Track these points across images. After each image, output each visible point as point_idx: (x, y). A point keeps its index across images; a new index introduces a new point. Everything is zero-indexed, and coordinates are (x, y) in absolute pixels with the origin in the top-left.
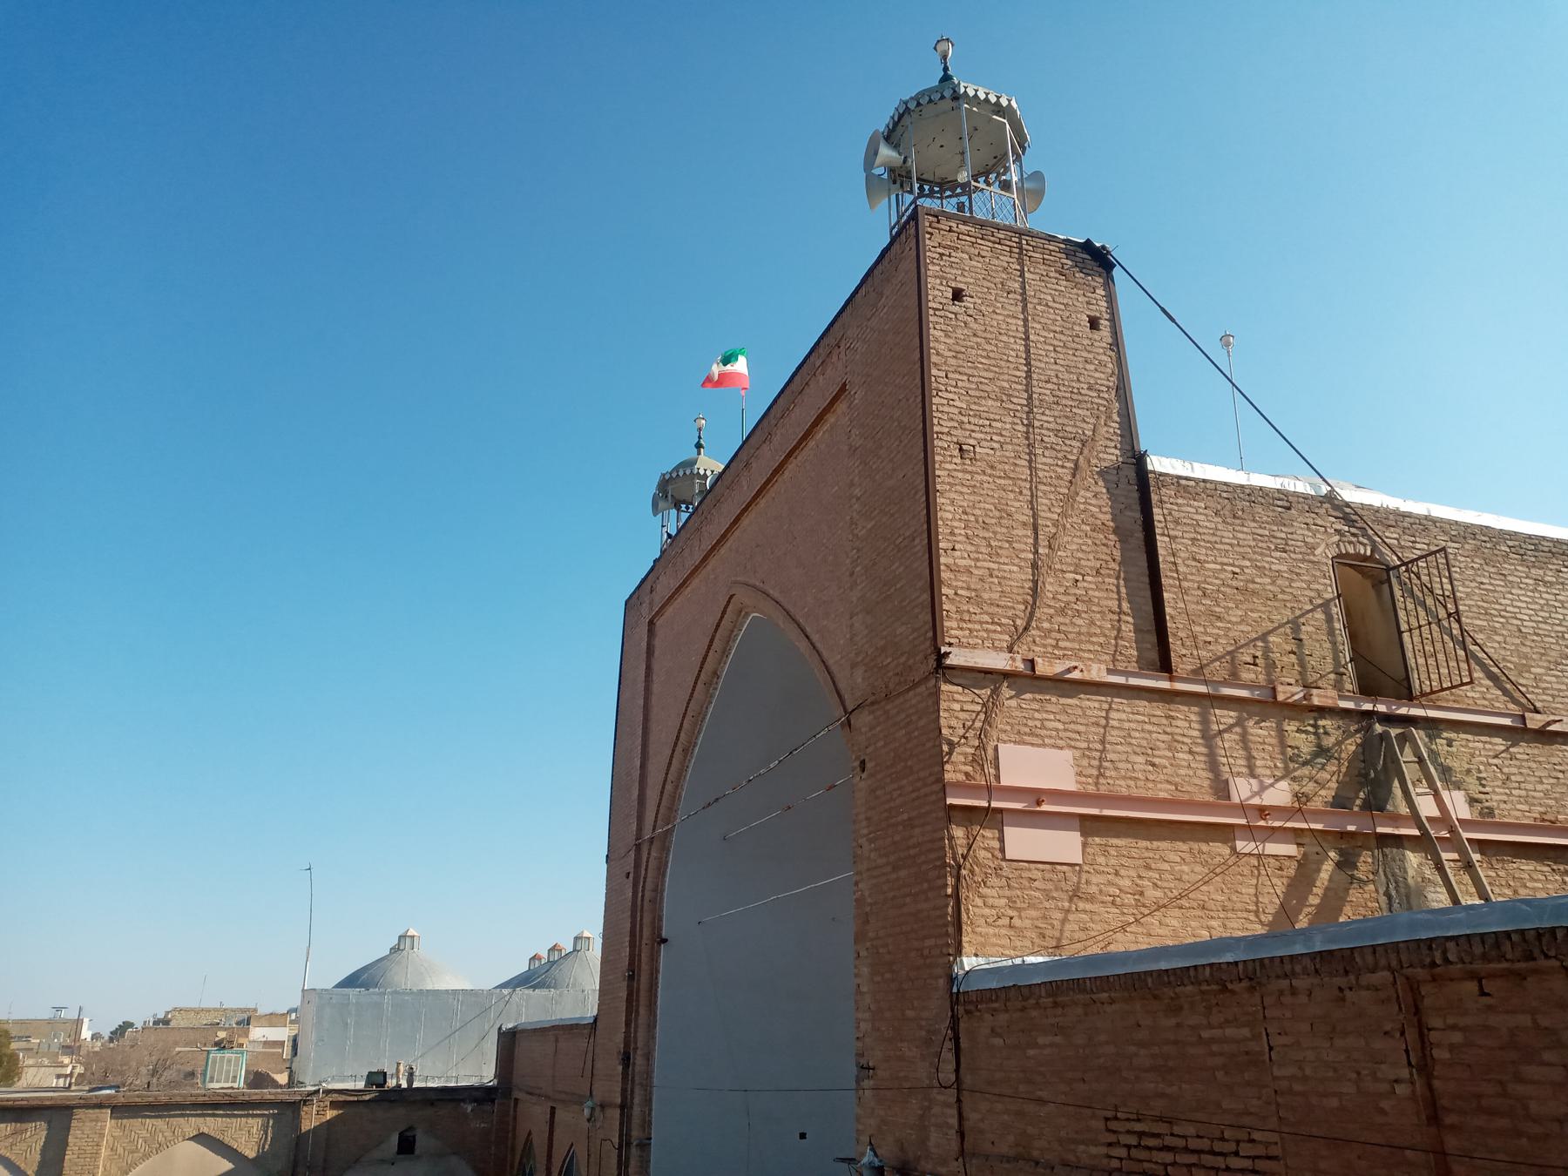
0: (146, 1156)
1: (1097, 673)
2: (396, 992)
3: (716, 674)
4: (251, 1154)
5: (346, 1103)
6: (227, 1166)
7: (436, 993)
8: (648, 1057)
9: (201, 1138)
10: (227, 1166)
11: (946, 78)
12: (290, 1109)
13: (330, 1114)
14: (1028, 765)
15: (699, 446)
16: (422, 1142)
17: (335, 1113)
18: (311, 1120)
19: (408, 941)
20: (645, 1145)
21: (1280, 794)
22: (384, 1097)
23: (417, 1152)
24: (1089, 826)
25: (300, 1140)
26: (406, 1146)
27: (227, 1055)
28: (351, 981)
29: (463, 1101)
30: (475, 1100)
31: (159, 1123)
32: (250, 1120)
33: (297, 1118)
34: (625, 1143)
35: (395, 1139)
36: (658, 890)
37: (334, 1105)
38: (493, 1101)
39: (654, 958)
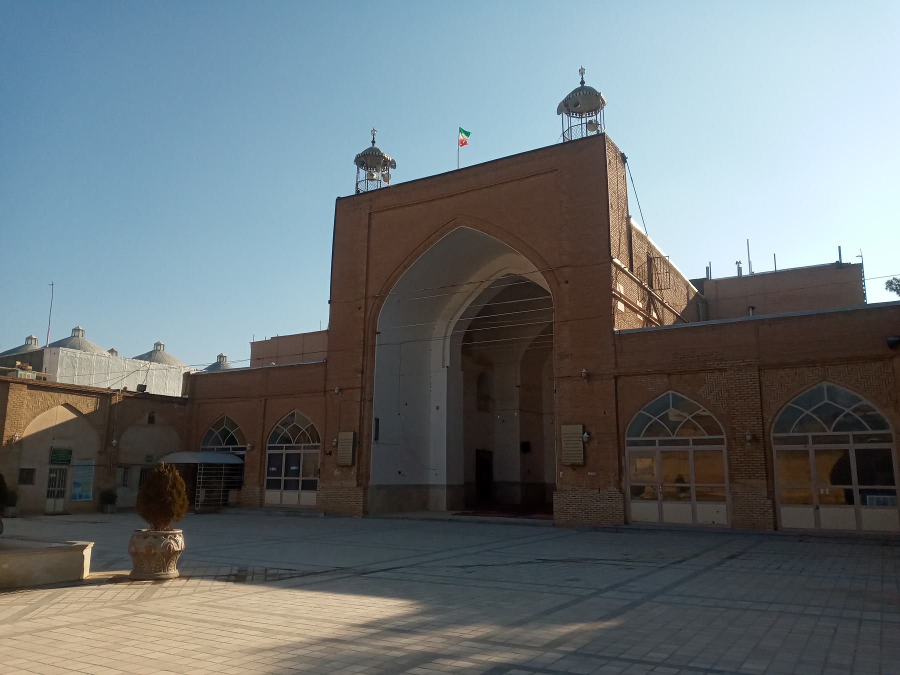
1: (626, 269)
3: (432, 243)
8: (372, 370)
9: (67, 405)
11: (582, 82)
12: (104, 396)
14: (620, 288)
15: (373, 142)
20: (371, 400)
21: (640, 305)
24: (626, 305)
26: (151, 420)
34: (363, 400)
35: (147, 416)
36: (376, 316)
38: (185, 404)
39: (374, 339)
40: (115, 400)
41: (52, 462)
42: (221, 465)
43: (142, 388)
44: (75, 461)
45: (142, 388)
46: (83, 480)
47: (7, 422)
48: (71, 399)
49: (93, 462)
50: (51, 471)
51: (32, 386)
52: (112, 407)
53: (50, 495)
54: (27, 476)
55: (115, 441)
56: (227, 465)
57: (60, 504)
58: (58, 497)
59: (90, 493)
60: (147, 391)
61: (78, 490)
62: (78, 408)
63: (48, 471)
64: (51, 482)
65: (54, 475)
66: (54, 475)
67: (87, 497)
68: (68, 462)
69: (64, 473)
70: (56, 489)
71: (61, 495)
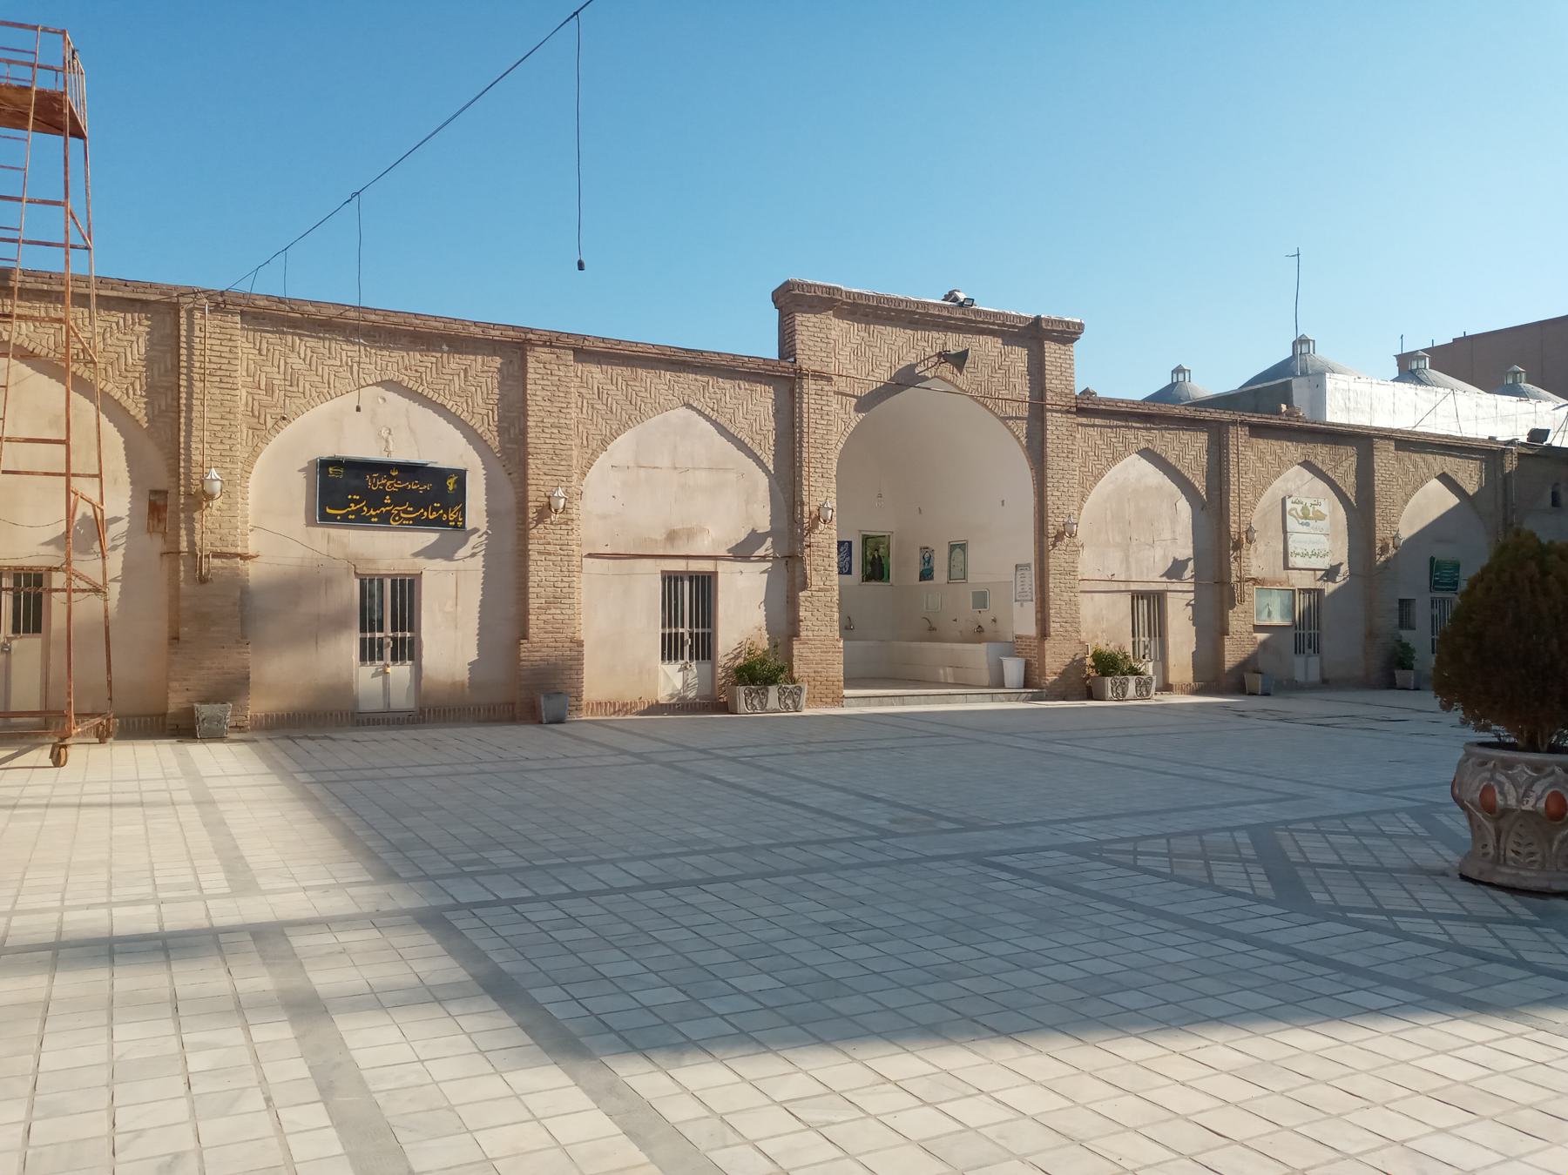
40: (1510, 464)
48: (1450, 464)
52: (1507, 477)
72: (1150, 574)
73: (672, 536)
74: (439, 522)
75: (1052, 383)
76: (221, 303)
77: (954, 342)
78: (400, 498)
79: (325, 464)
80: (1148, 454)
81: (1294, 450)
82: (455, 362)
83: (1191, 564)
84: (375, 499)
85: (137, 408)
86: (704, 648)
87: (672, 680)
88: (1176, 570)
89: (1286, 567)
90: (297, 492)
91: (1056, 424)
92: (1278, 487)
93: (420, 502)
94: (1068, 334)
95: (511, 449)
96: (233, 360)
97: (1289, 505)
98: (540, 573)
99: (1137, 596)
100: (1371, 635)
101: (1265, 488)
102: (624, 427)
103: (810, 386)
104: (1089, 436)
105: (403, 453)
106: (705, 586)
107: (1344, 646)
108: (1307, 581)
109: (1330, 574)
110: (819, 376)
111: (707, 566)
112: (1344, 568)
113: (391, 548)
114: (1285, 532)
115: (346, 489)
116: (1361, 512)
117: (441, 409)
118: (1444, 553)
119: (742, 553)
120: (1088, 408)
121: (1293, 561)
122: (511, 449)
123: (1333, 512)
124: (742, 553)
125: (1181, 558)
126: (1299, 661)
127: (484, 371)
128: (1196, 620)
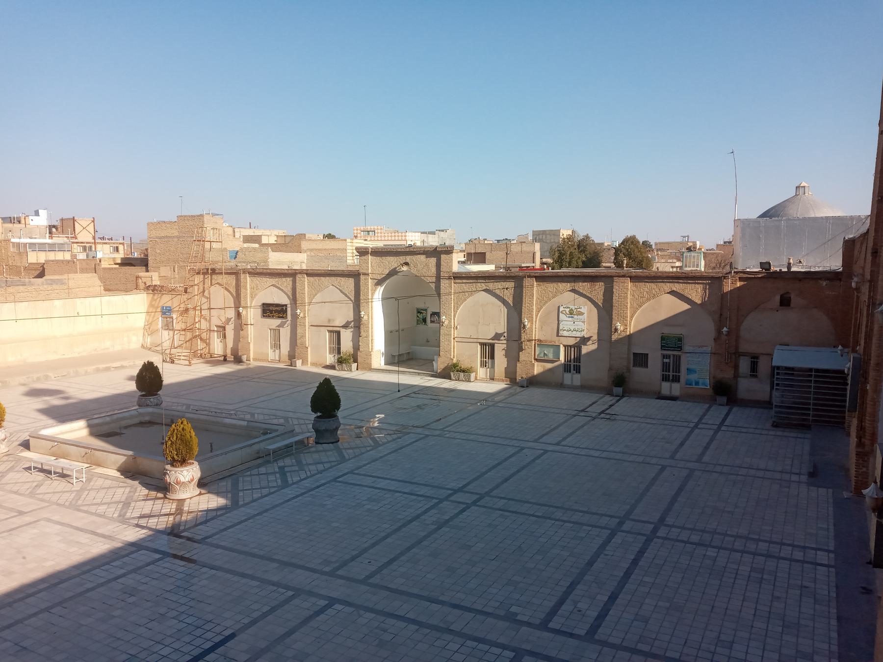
0: (648, 300)
2: (789, 219)
4: (699, 302)
5: (748, 277)
6: (686, 306)
7: (815, 219)
9: (672, 293)
10: (686, 306)
13: (739, 284)
16: (795, 300)
17: (742, 283)
18: (728, 286)
19: (801, 190)
22: (768, 275)
23: (792, 305)
25: (724, 296)
26: (785, 302)
27: (693, 254)
28: (764, 215)
29: (820, 279)
30: (828, 279)
31: (652, 285)
32: (697, 286)
33: (721, 286)
37: (741, 279)
41: (663, 347)
42: (811, 370)
43: (765, 266)
44: (687, 348)
45: (765, 266)
46: (699, 368)
47: (614, 312)
48: (677, 287)
49: (709, 349)
50: (664, 356)
51: (634, 279)
53: (665, 378)
54: (641, 360)
55: (725, 329)
56: (817, 370)
57: (676, 389)
58: (673, 381)
59: (705, 383)
60: (773, 269)
61: (693, 377)
62: (686, 295)
63: (660, 358)
64: (665, 367)
65: (667, 360)
66: (667, 360)
67: (704, 384)
68: (680, 348)
69: (678, 359)
70: (671, 372)
71: (676, 379)
72: (487, 335)
73: (329, 321)
74: (282, 317)
75: (443, 269)
76: (245, 271)
77: (408, 259)
78: (276, 311)
79: (263, 304)
80: (486, 291)
81: (562, 286)
82: (284, 279)
83: (505, 334)
84: (271, 312)
85: (234, 293)
86: (339, 353)
87: (330, 359)
88: (497, 337)
89: (558, 335)
90: (259, 311)
91: (444, 284)
92: (556, 301)
93: (279, 312)
94: (449, 251)
95: (294, 299)
96: (248, 281)
97: (561, 309)
98: (299, 330)
99: (483, 345)
100: (610, 369)
101: (546, 302)
102: (318, 292)
103: (362, 277)
104: (454, 287)
105: (276, 301)
106: (338, 333)
107: (597, 372)
108: (572, 342)
109: (584, 340)
110: (365, 274)
111: (338, 329)
112: (595, 337)
113: (275, 322)
114: (558, 320)
115: (270, 310)
116: (606, 312)
117: (282, 290)
118: (667, 331)
119: (345, 326)
120: (457, 277)
121: (561, 333)
122: (294, 299)
123: (590, 311)
124: (345, 326)
125: (500, 332)
126: (568, 376)
127: (289, 280)
128: (506, 356)
